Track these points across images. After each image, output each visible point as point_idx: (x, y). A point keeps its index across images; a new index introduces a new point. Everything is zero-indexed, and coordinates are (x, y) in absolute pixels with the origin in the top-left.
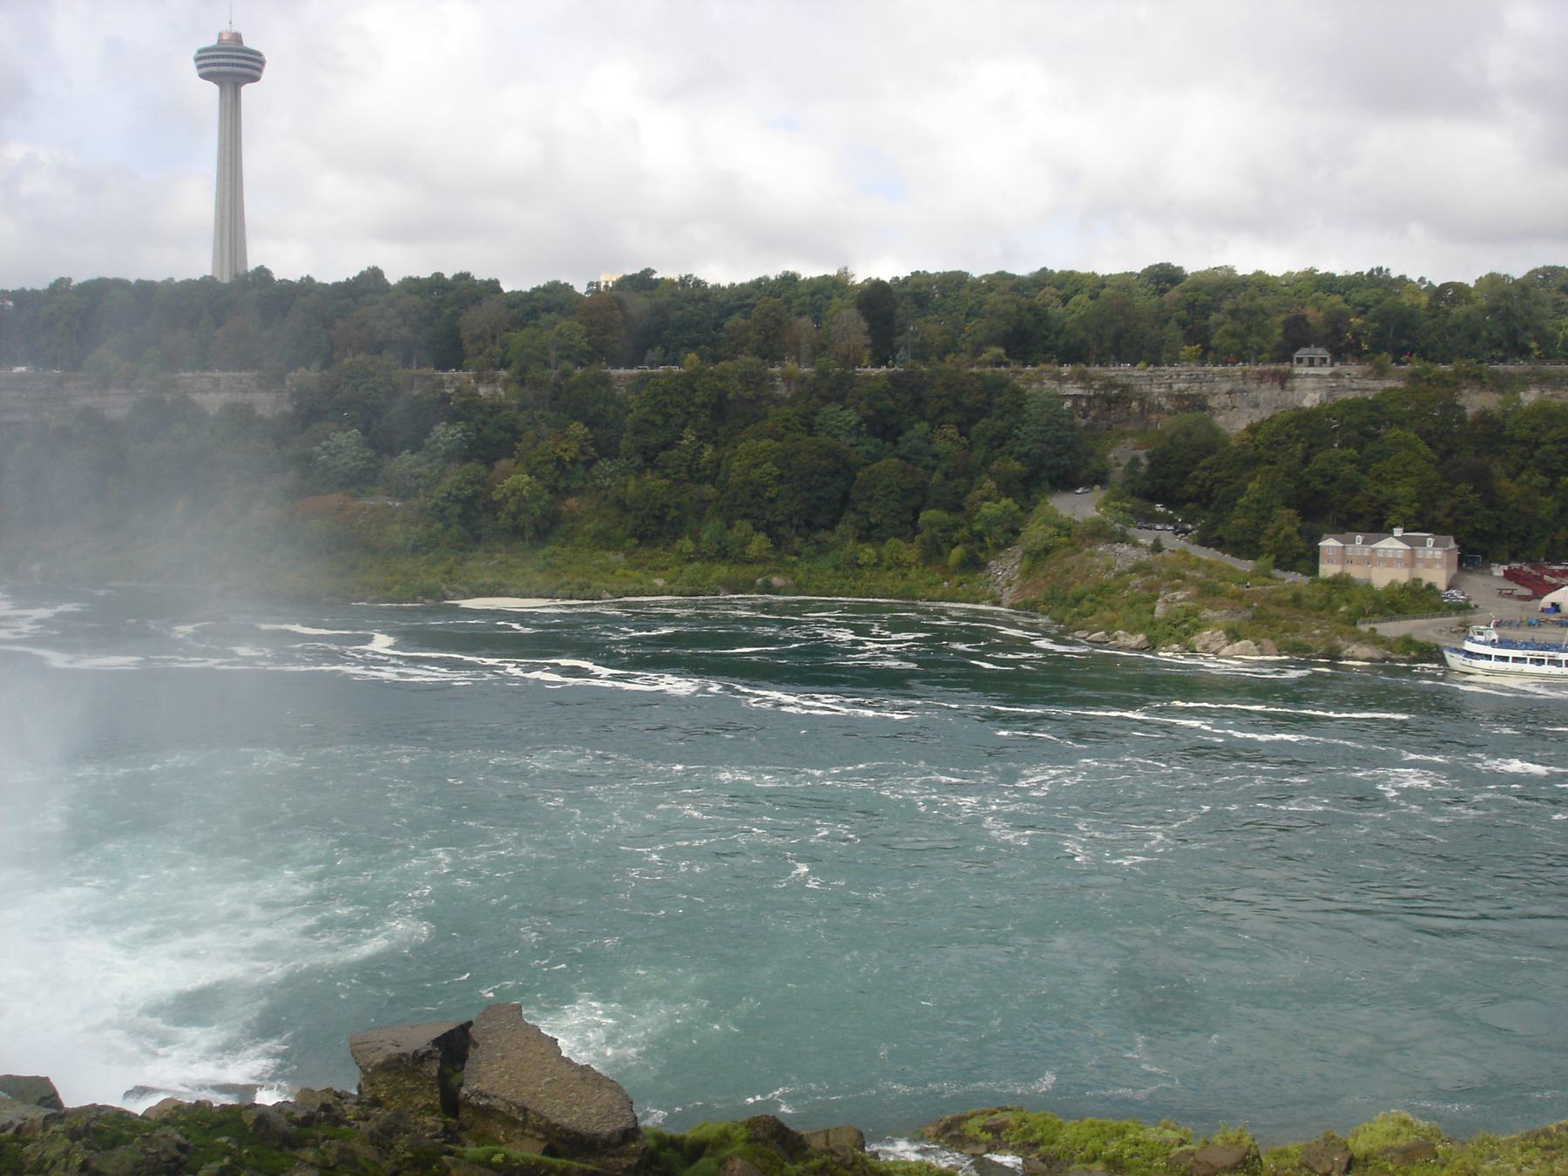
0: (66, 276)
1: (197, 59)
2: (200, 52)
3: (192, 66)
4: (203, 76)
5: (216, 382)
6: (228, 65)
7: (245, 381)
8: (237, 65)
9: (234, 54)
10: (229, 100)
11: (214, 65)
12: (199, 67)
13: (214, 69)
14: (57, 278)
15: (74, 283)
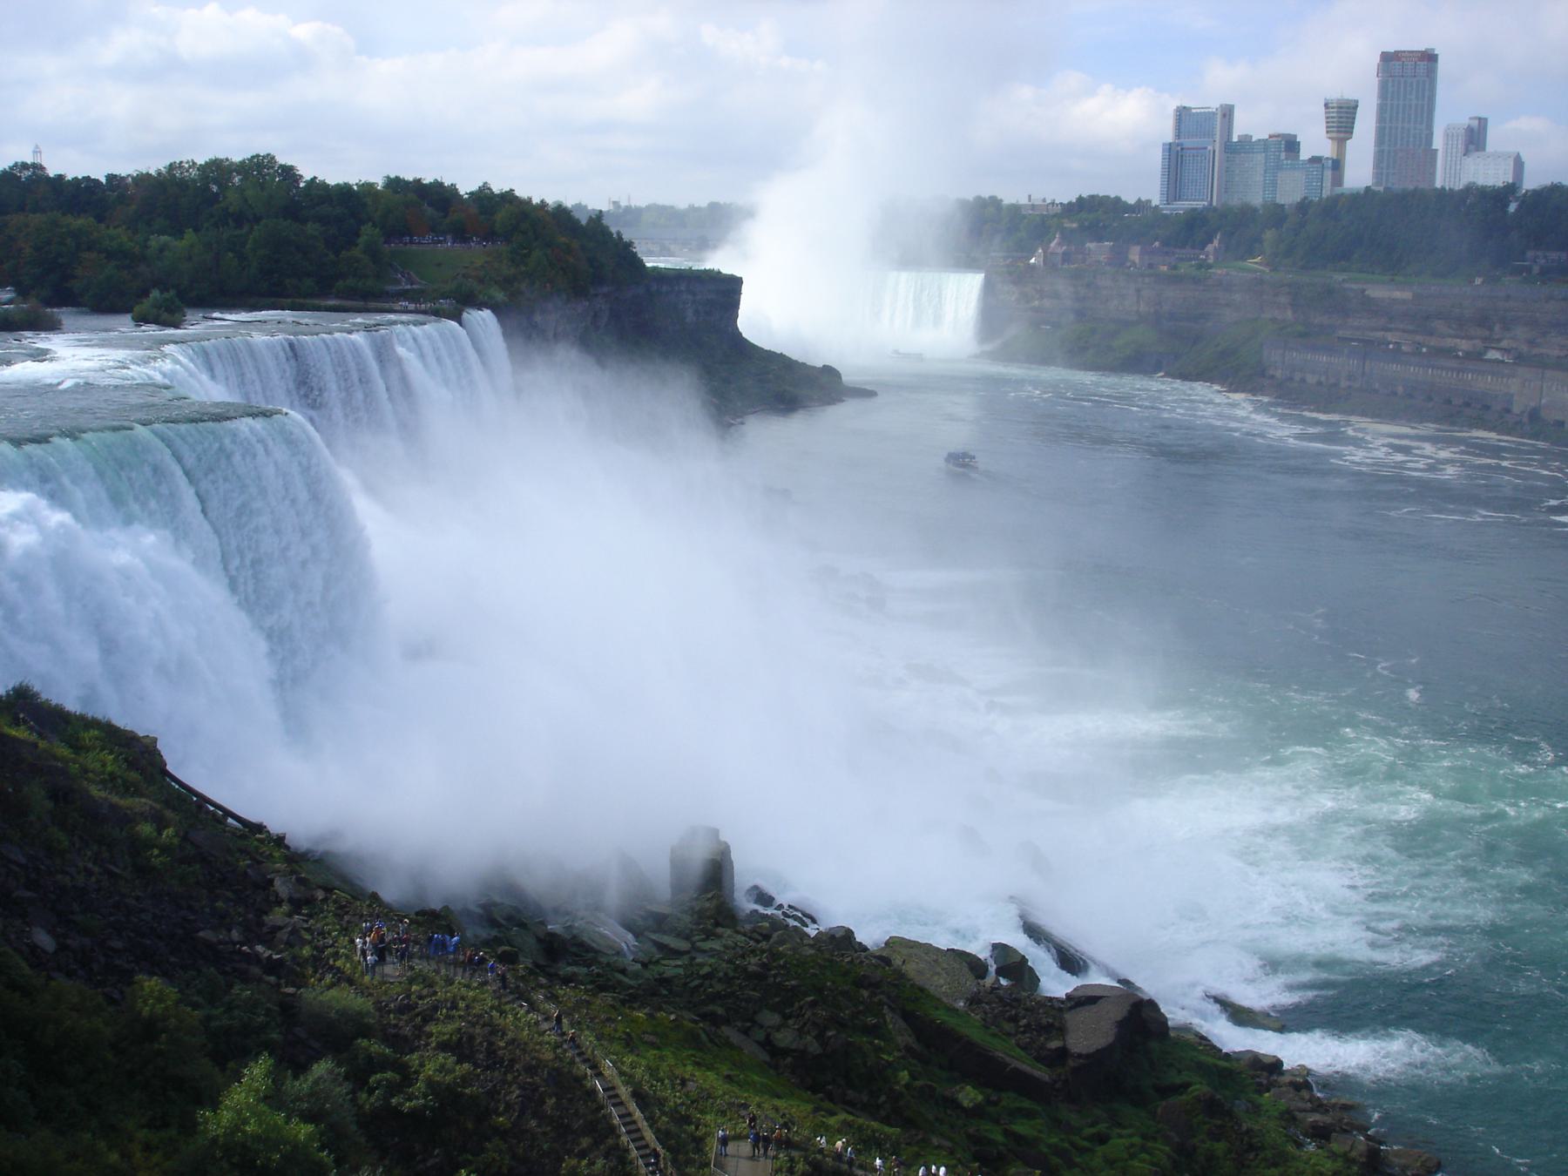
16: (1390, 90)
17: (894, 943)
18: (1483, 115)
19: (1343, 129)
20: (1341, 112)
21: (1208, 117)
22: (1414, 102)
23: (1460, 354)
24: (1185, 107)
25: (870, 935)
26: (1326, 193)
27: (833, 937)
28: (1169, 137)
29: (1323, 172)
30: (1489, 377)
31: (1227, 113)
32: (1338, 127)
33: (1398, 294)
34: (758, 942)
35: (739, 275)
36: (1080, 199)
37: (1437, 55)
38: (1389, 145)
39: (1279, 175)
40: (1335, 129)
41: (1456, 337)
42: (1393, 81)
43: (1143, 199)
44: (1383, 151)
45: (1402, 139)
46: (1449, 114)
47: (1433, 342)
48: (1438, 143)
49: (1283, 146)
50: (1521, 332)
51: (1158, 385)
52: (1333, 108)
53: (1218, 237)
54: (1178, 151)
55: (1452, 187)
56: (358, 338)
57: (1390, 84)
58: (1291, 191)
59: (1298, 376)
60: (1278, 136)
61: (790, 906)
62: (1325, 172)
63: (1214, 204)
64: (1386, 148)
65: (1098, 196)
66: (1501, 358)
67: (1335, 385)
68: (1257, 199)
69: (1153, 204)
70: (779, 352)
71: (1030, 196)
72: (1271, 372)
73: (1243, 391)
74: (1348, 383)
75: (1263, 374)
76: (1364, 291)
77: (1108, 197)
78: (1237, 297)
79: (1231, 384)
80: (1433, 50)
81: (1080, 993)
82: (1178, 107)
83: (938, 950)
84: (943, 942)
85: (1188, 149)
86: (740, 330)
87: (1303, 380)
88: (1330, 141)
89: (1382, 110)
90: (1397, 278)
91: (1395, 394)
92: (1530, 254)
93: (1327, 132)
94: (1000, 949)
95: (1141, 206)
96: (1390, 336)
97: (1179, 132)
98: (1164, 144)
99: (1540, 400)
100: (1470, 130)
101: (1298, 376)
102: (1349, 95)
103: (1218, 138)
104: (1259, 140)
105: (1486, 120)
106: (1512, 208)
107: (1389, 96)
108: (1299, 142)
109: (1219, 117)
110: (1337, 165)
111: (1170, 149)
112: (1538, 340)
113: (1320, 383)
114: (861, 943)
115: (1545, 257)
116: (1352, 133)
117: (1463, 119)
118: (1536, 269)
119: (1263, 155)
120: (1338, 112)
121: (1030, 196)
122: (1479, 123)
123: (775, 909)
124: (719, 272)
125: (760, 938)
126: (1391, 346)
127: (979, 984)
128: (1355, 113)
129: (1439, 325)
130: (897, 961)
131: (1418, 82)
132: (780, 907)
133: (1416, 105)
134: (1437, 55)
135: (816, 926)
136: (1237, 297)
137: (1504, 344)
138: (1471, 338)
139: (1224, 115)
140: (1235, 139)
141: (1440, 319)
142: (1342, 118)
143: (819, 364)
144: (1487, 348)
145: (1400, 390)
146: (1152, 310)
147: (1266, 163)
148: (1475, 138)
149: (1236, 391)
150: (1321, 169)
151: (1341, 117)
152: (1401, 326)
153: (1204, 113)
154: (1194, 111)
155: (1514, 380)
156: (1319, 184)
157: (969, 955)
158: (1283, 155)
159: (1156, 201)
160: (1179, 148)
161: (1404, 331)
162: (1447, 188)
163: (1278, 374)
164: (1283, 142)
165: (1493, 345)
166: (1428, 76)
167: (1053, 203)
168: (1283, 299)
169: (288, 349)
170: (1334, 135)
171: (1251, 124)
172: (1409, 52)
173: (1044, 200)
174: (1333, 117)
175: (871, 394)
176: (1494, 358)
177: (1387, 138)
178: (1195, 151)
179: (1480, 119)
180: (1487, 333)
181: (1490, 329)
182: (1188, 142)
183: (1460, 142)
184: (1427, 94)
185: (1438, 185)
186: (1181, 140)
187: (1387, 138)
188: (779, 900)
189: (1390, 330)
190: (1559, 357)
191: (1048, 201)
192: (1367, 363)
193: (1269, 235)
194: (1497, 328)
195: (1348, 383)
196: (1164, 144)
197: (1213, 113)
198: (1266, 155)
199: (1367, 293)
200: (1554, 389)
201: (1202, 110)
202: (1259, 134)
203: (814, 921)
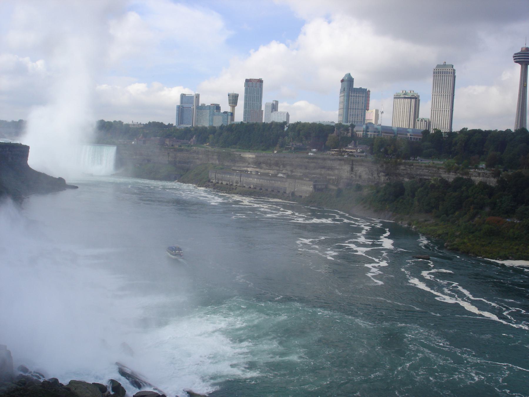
0: (466, 128)
1: (514, 57)
2: (515, 54)
3: (513, 59)
4: (516, 62)
5: (479, 174)
6: (523, 58)
7: (488, 174)
8: (526, 59)
9: (527, 55)
10: (523, 70)
11: (518, 59)
12: (514, 59)
13: (518, 60)
14: (463, 128)
15: (468, 130)
16: (248, 91)
17: (72, 383)
18: (277, 100)
19: (234, 103)
20: (233, 98)
21: (191, 97)
22: (256, 95)
23: (270, 175)
24: (184, 94)
25: (65, 381)
26: (229, 123)
27: (49, 382)
28: (179, 104)
29: (228, 116)
30: (279, 182)
31: (198, 96)
32: (232, 102)
33: (251, 156)
34: (20, 386)
35: (28, 145)
36: (150, 123)
38: (248, 109)
39: (214, 117)
40: (232, 103)
41: (269, 169)
42: (249, 88)
43: (170, 123)
44: (246, 110)
45: (252, 106)
46: (267, 99)
47: (262, 171)
48: (263, 108)
49: (215, 108)
50: (288, 168)
51: (175, 184)
52: (231, 96)
53: (195, 137)
54: (182, 108)
55: (268, 122)
57: (248, 89)
58: (218, 122)
59: (220, 182)
60: (214, 104)
61: (34, 372)
62: (228, 117)
63: (194, 126)
64: (247, 109)
65: (155, 122)
66: (283, 176)
67: (231, 185)
68: (206, 124)
69: (174, 125)
72: (212, 181)
73: (203, 187)
74: (236, 184)
75: (209, 181)
76: (240, 155)
77: (159, 122)
78: (201, 156)
79: (199, 185)
80: (262, 79)
81: (138, 395)
82: (181, 94)
83: (88, 384)
84: (91, 381)
85: (185, 107)
86: (29, 165)
87: (222, 183)
88: (230, 107)
89: (246, 97)
90: (251, 151)
91: (250, 187)
92: (291, 144)
93: (229, 104)
94: (112, 381)
95: (170, 126)
96: (249, 169)
97: (182, 102)
98: (177, 106)
99: (295, 190)
100: (273, 104)
101: (220, 182)
103: (194, 105)
104: (208, 106)
105: (278, 101)
106: (286, 129)
107: (248, 93)
108: (220, 107)
109: (195, 97)
110: (232, 114)
111: (179, 108)
112: (294, 170)
113: (227, 184)
114: (61, 383)
115: (295, 144)
116: (237, 104)
118: (293, 148)
119: (209, 110)
120: (232, 97)
121: (133, 121)
122: (276, 102)
123: (29, 374)
124: (21, 144)
125: (22, 385)
126: (249, 172)
127: (103, 395)
128: (238, 98)
129: (263, 166)
130: (73, 389)
131: (257, 88)
132: (31, 372)
133: (257, 96)
134: (263, 81)
135: (44, 379)
136: (201, 156)
137: (284, 172)
138: (273, 170)
139: (196, 97)
140: (200, 105)
141: (264, 164)
142: (234, 99)
143: (57, 177)
144: (278, 173)
145: (252, 186)
146: (173, 160)
147: (210, 113)
148: (274, 107)
149: (200, 187)
150: (227, 116)
151: (233, 99)
152: (252, 166)
153: (190, 96)
154: (187, 95)
155: (287, 183)
156: (227, 120)
157: (98, 384)
158: (215, 111)
159: (174, 125)
160: (182, 107)
161: (253, 167)
162: (266, 123)
163: (214, 181)
164: (215, 107)
165: (280, 172)
166: (260, 87)
167: (140, 124)
168: (215, 157)
170: (231, 105)
171: (206, 100)
172: (254, 79)
173: (137, 123)
174: (231, 99)
175: (77, 187)
176: (280, 176)
177: (248, 106)
178: (186, 108)
179: (276, 101)
180: (278, 168)
181: (279, 167)
182: (185, 105)
183: (270, 108)
184: (260, 93)
185: (263, 122)
186: (182, 105)
187: (248, 106)
188: (30, 369)
189: (248, 167)
190: (300, 176)
191: (139, 123)
192: (242, 178)
193: (211, 136)
194: (281, 166)
195: (236, 184)
196: (177, 106)
197: (193, 96)
198: (210, 111)
199: (241, 155)
200: (299, 185)
201: (189, 95)
202: (208, 103)
203: (43, 377)
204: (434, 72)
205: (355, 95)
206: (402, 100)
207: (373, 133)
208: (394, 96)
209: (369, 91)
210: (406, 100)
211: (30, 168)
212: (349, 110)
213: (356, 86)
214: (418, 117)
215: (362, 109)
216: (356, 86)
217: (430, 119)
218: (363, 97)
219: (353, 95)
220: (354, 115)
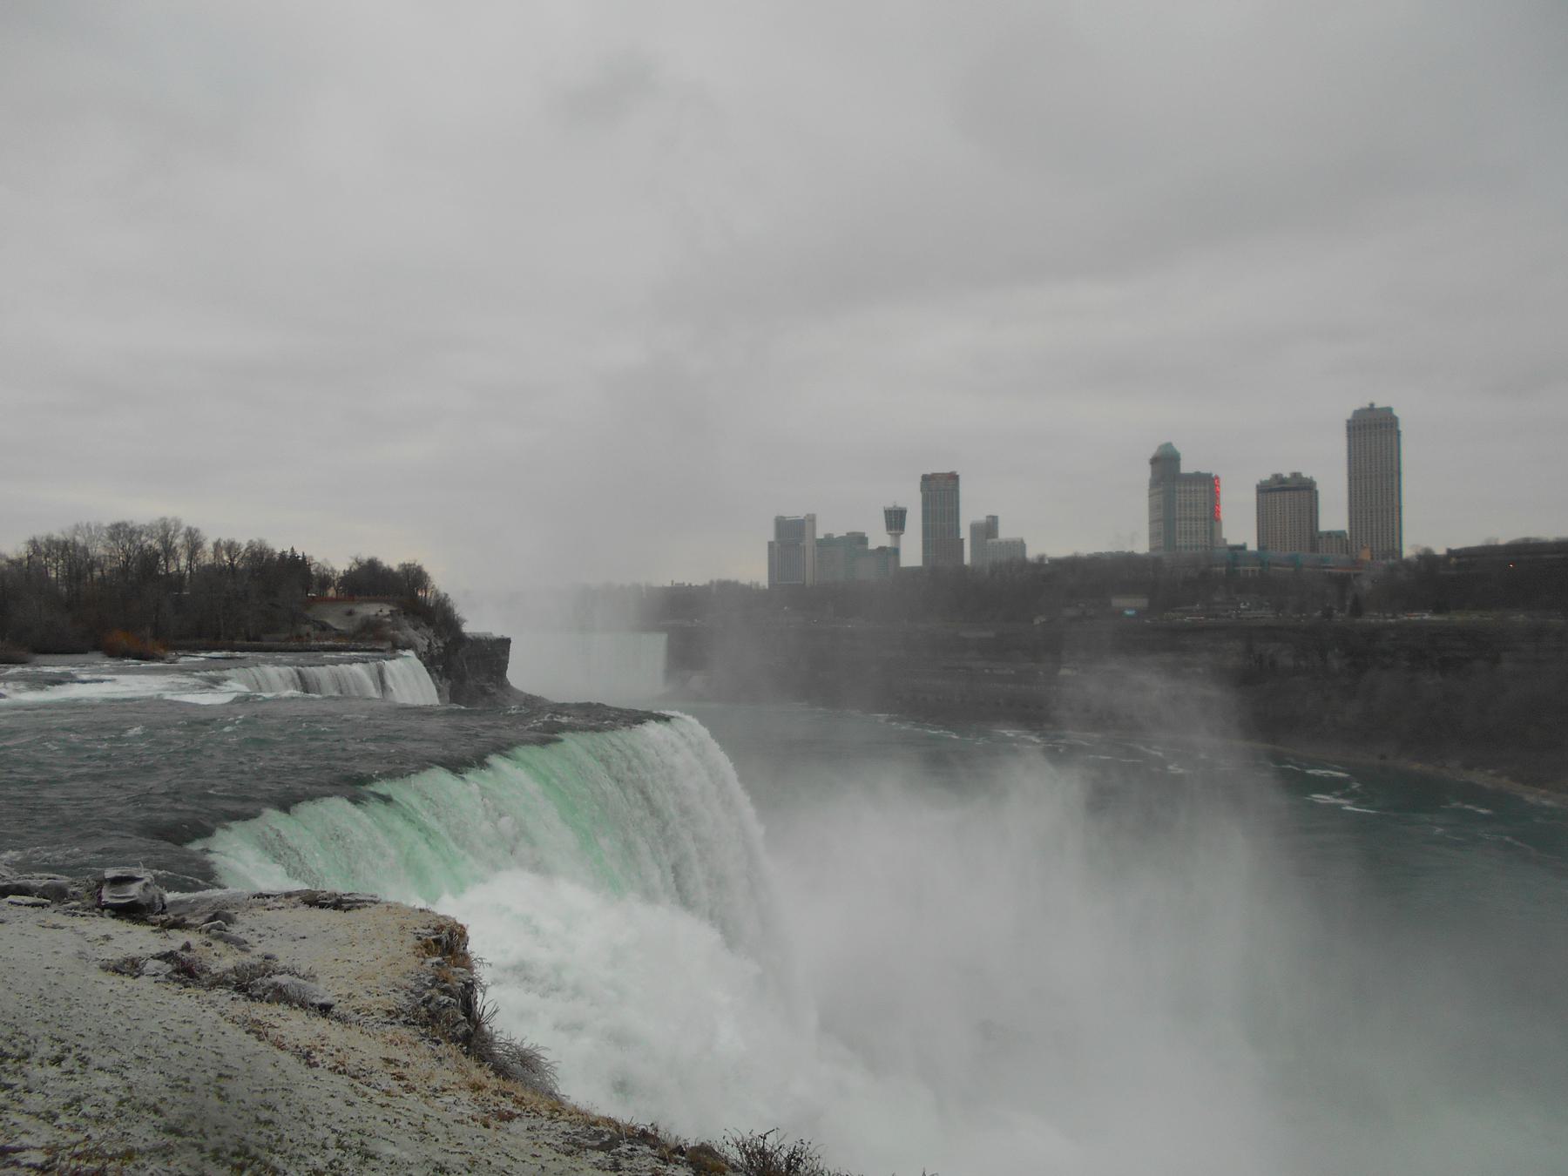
28: (772, 538)
31: (812, 519)
37: (958, 476)
46: (970, 514)
48: (965, 533)
56: (357, 668)
60: (854, 533)
70: (538, 695)
71: (672, 582)
88: (889, 536)
98: (769, 543)
102: (901, 505)
110: (896, 552)
117: (981, 518)
121: (672, 582)
134: (958, 476)
140: (820, 535)
142: (896, 519)
148: (989, 528)
154: (787, 519)
167: (690, 585)
169: (296, 676)
171: (831, 525)
173: (684, 584)
191: (687, 584)
202: (839, 532)
204: (1349, 429)
205: (1188, 488)
206: (1278, 494)
207: (1257, 568)
208: (1258, 486)
209: (1217, 478)
210: (1287, 493)
211: (512, 687)
212: (1177, 523)
213: (1186, 467)
214: (1317, 527)
215: (1205, 519)
216: (1186, 467)
217: (1347, 532)
218: (1205, 491)
219: (1182, 488)
220: (1188, 533)
